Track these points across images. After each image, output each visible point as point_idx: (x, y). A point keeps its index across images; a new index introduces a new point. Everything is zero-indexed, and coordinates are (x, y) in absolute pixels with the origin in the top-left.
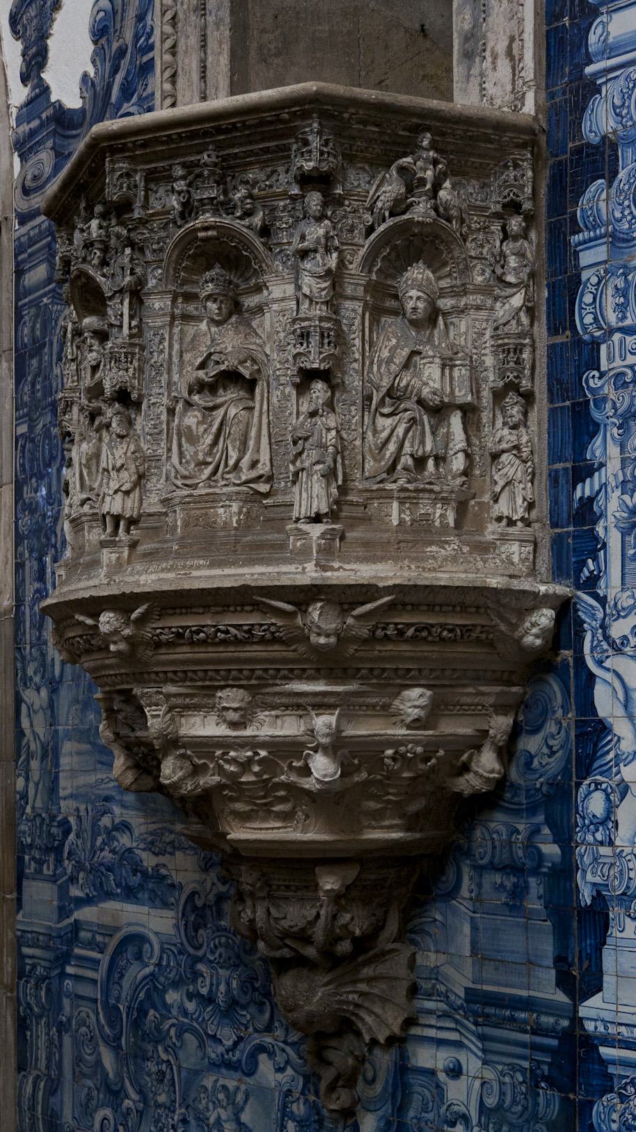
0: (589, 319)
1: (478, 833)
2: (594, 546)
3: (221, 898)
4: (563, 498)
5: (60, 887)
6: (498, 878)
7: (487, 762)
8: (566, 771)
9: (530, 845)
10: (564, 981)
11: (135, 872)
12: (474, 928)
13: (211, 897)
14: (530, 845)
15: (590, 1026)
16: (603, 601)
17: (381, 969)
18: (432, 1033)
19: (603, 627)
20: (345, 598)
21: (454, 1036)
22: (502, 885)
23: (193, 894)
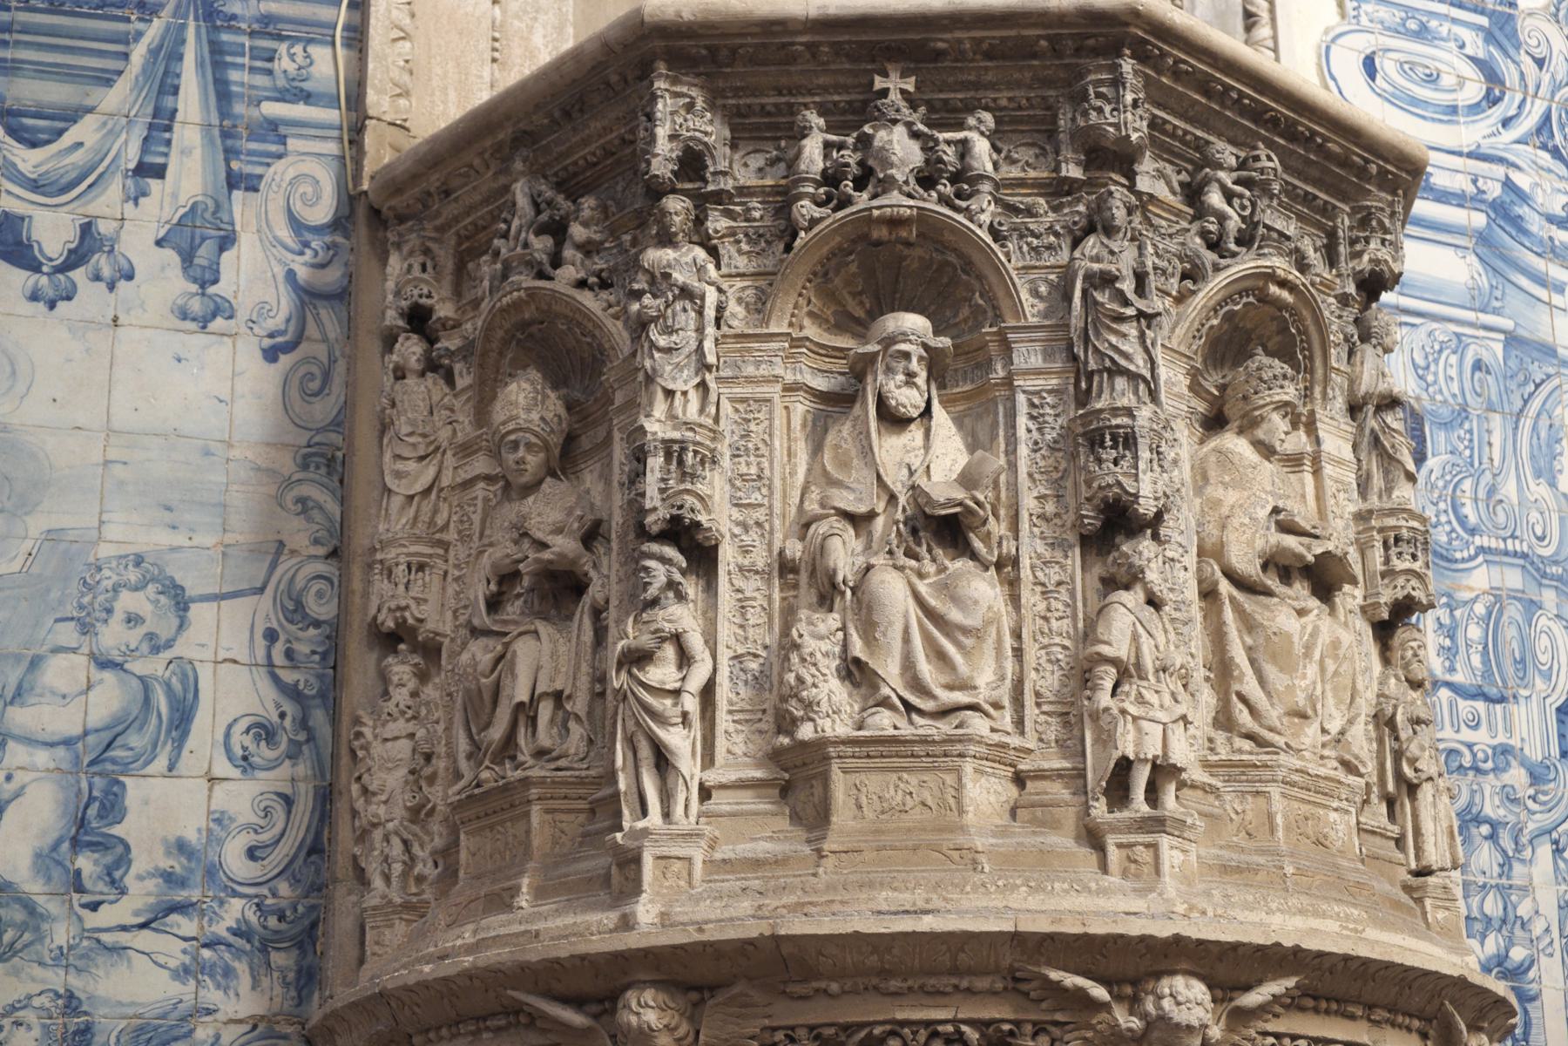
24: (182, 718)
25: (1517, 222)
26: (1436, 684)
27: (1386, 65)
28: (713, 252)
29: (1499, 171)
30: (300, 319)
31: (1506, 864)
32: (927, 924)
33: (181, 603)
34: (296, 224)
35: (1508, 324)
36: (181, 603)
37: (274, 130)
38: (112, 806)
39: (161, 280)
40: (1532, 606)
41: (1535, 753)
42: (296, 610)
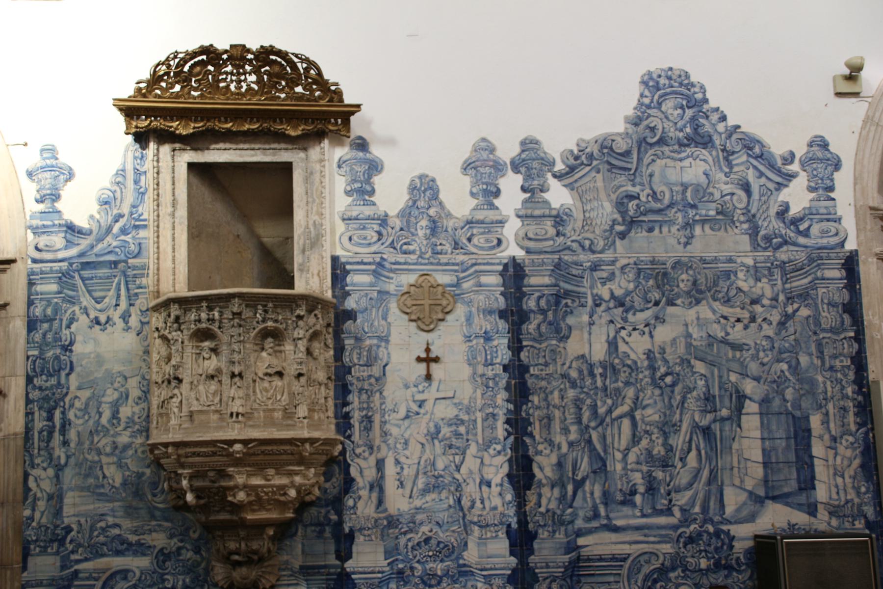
0: (348, 360)
1: (305, 514)
2: (350, 426)
3: (179, 549)
4: (339, 411)
5: (62, 557)
6: (313, 528)
7: (317, 492)
8: (340, 493)
9: (326, 516)
10: (339, 557)
11: (122, 544)
12: (303, 545)
13: (174, 549)
14: (326, 516)
15: (348, 570)
16: (353, 442)
17: (271, 562)
18: (286, 582)
19: (353, 450)
20: (312, 441)
21: (295, 582)
22: (315, 531)
23: (162, 550)
24: (127, 397)
25: (383, 266)
26: (355, 365)
27: (355, 238)
28: (182, 332)
29: (380, 255)
30: (142, 328)
31: (369, 397)
32: (201, 439)
33: (126, 378)
34: (141, 311)
35: (378, 288)
36: (126, 378)
37: (136, 294)
38: (118, 412)
39: (120, 324)
40: (379, 346)
41: (377, 375)
42: (144, 378)
